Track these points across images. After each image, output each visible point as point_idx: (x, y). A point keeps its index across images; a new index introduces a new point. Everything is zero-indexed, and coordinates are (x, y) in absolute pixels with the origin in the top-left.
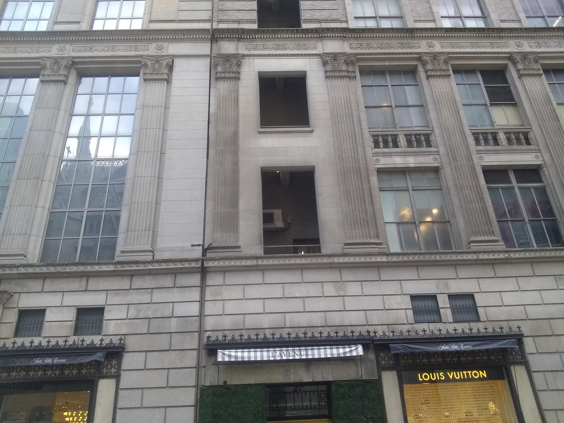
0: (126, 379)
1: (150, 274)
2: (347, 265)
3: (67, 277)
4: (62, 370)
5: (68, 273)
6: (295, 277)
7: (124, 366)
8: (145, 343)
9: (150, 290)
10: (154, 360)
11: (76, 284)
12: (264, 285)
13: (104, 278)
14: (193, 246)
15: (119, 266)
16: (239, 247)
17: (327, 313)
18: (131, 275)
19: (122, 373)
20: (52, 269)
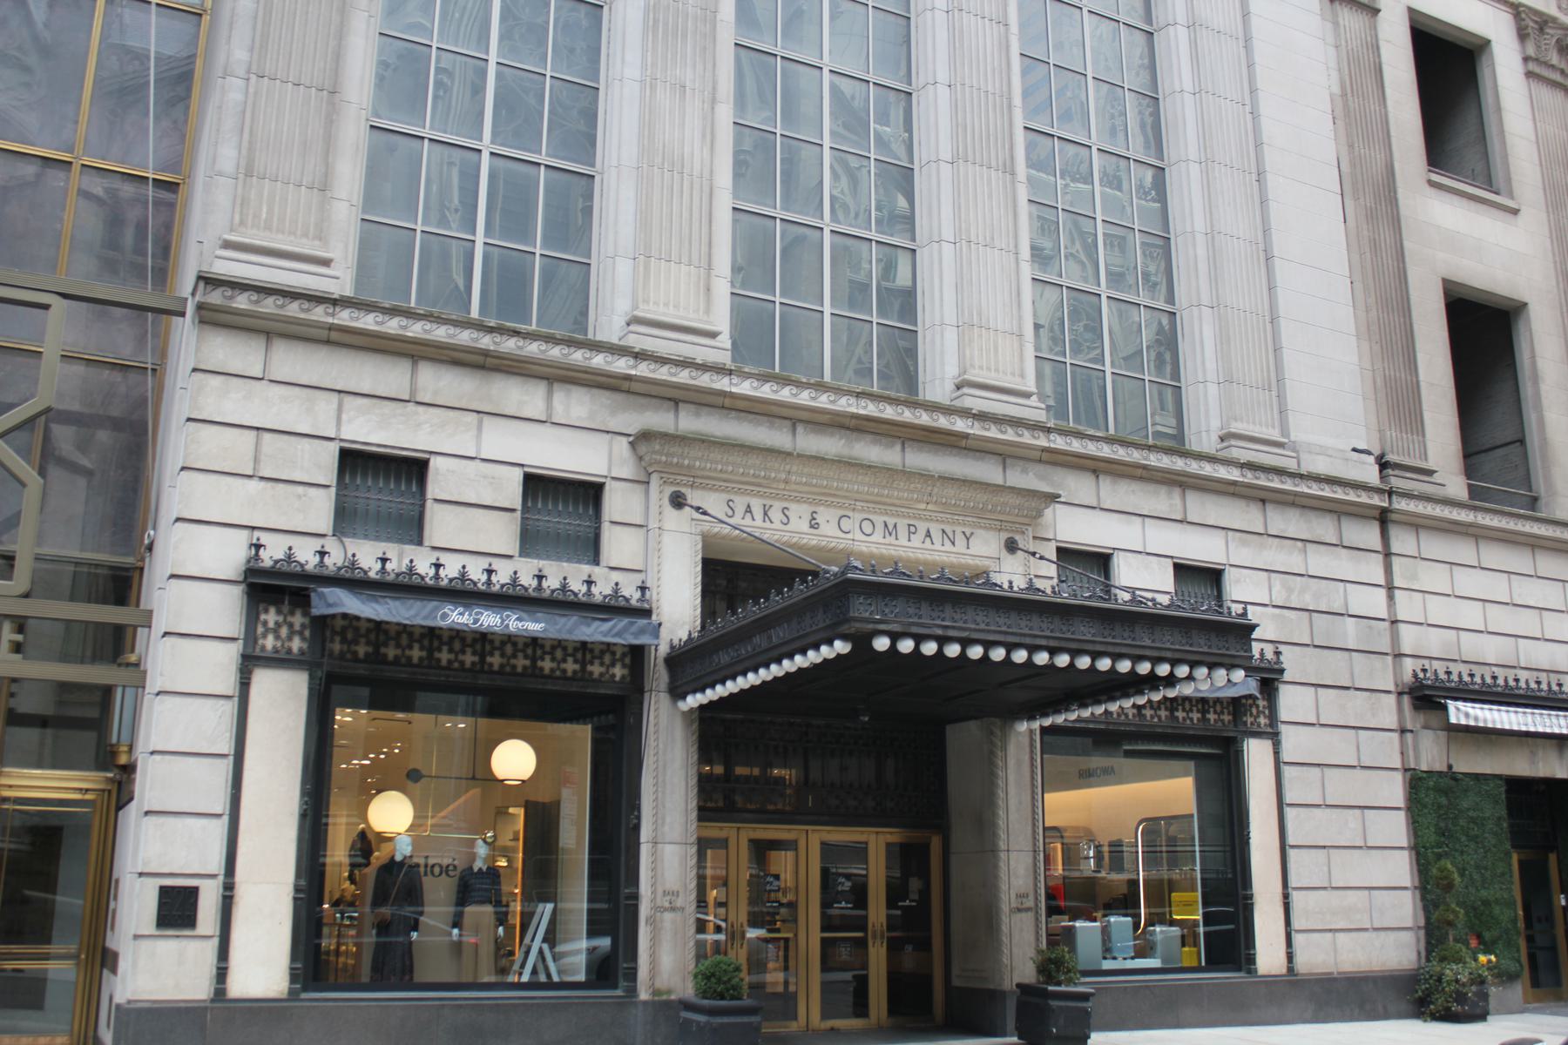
0: (1294, 742)
1: (1293, 504)
2: (1549, 544)
3: (1141, 478)
4: (1204, 712)
5: (1145, 467)
6: (1517, 560)
7: (1284, 714)
8: (1334, 668)
9: (1299, 544)
10: (1333, 707)
11: (1162, 501)
12: (1478, 571)
13: (1214, 498)
14: (1354, 450)
15: (1249, 474)
16: (1430, 473)
17: (1520, 641)
18: (1263, 498)
19: (1283, 728)
20: (1121, 453)
